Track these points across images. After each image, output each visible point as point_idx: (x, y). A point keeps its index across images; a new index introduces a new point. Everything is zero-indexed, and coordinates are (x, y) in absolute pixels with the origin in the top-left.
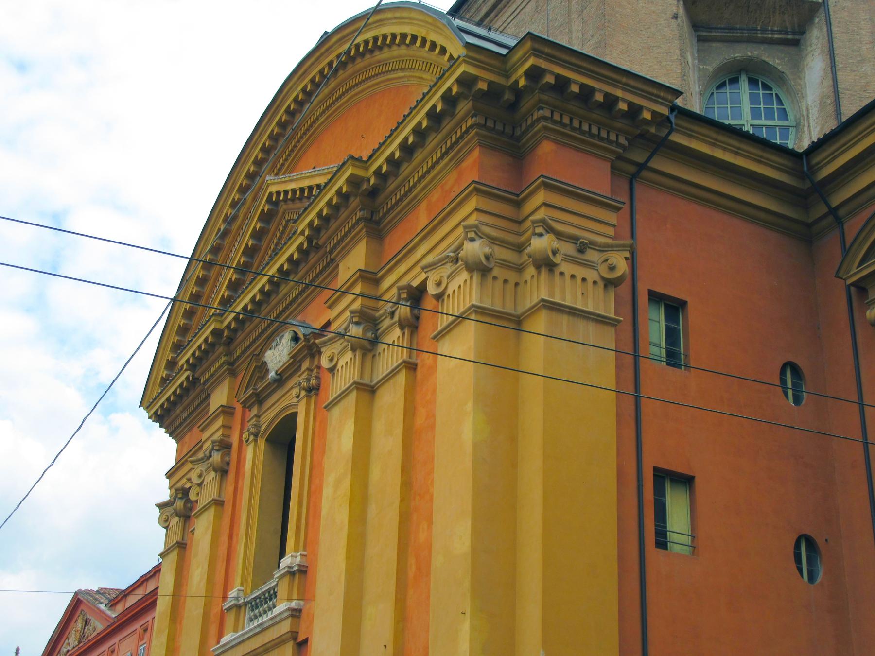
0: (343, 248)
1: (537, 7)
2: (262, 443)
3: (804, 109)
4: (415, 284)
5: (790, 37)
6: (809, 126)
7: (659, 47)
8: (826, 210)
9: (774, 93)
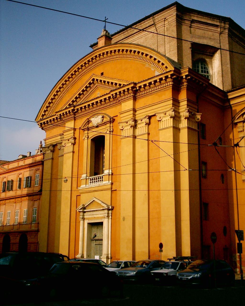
0: (125, 100)
1: (153, 36)
2: (90, 140)
3: (213, 72)
4: (150, 115)
5: (211, 54)
6: (215, 77)
7: (187, 55)
8: (229, 104)
9: (206, 66)
